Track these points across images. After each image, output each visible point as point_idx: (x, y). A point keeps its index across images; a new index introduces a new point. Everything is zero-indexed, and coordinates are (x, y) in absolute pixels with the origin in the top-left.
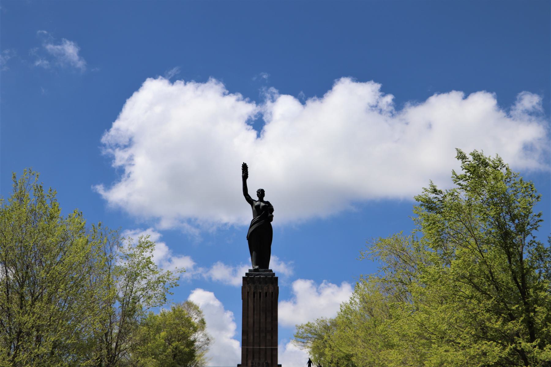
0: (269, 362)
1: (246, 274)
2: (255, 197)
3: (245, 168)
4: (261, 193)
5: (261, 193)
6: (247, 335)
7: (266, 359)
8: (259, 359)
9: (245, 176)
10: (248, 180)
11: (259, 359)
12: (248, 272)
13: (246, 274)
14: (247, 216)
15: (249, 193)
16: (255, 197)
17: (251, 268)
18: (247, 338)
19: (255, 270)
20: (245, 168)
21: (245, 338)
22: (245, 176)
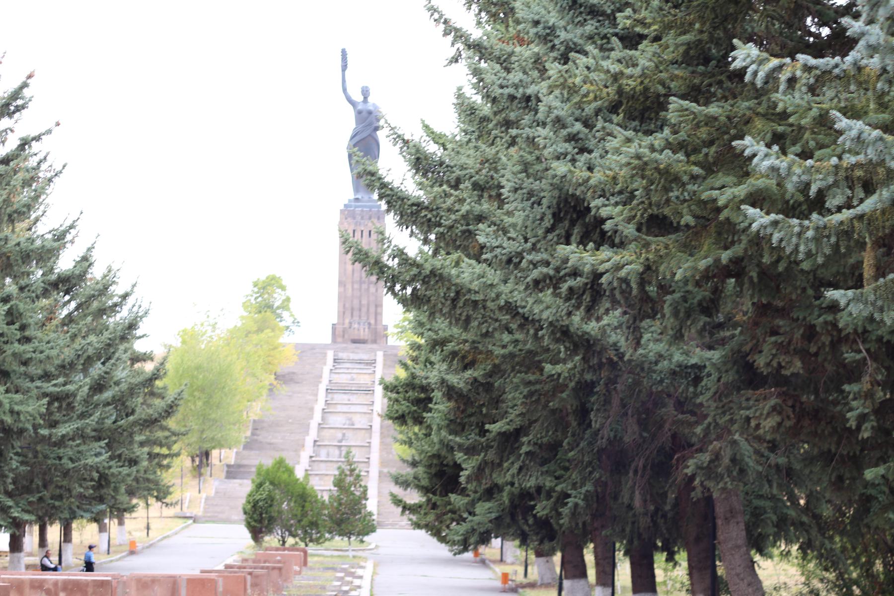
0: (372, 322)
1: (345, 206)
2: (358, 97)
3: (344, 53)
4: (365, 93)
5: (365, 93)
6: (345, 286)
7: (368, 319)
8: (360, 317)
9: (344, 67)
10: (346, 72)
11: (360, 317)
12: (347, 202)
13: (345, 206)
14: (348, 124)
15: (349, 91)
16: (358, 97)
17: (352, 197)
18: (345, 290)
19: (357, 200)
20: (344, 53)
21: (342, 290)
22: (344, 67)
